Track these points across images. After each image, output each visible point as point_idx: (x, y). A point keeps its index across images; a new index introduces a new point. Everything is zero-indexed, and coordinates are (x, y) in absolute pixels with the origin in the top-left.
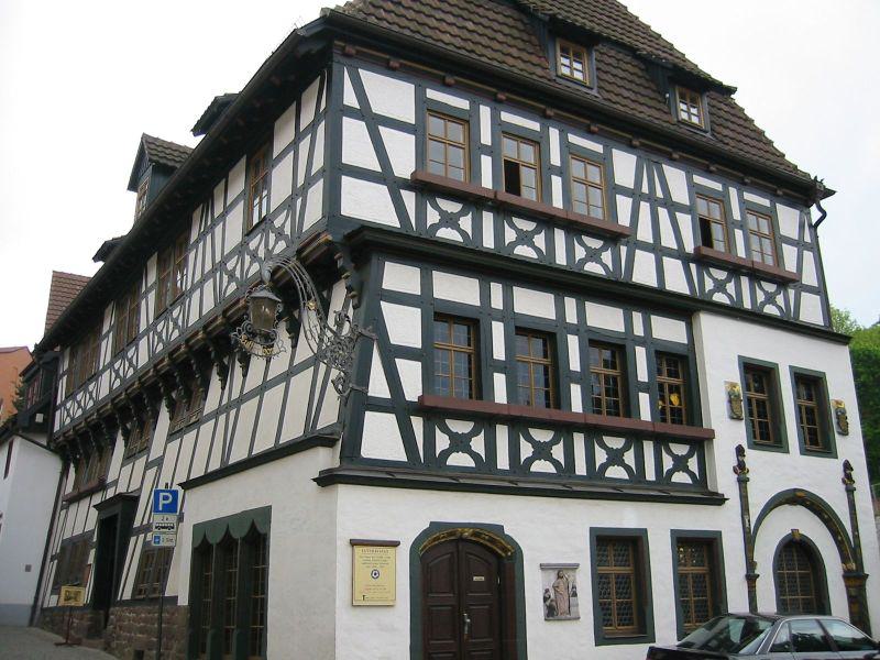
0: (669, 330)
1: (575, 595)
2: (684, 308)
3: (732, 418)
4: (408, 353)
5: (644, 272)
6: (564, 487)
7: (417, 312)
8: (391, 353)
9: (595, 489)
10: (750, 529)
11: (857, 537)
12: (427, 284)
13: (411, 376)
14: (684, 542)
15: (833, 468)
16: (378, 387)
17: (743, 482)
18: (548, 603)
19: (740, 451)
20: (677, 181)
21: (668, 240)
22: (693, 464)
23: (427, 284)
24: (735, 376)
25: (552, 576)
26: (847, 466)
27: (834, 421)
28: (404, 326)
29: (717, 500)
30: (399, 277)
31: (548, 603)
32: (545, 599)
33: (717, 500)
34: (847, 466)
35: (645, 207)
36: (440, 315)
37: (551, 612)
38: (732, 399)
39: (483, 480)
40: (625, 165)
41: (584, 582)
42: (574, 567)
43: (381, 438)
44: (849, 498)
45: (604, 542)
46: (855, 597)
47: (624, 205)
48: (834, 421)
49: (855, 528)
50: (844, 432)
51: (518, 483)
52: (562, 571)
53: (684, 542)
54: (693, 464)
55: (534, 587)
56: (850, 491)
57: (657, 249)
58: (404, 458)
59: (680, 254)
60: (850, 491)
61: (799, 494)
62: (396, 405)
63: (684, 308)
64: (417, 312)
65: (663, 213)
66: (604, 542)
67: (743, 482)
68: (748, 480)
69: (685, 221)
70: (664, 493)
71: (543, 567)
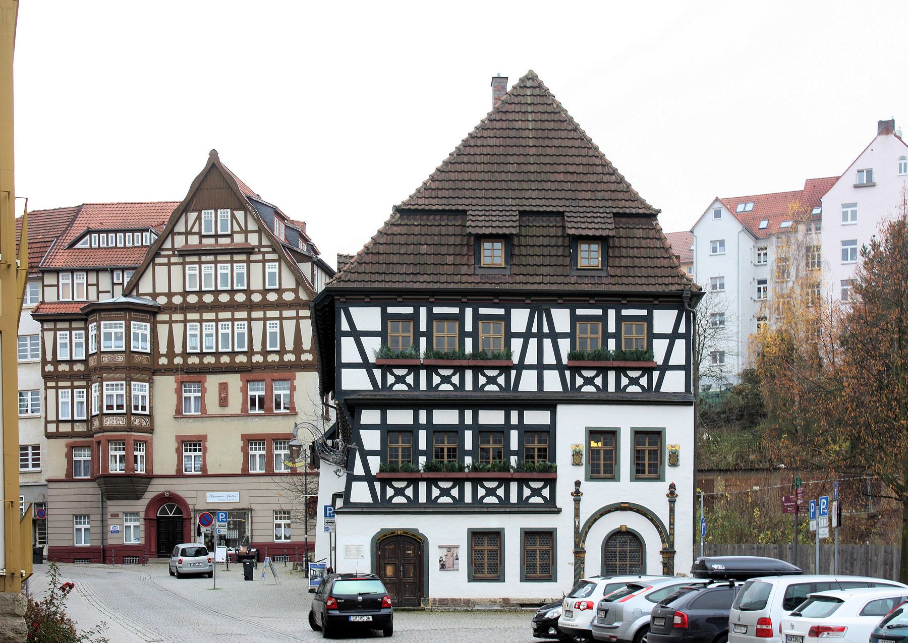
0: (536, 418)
1: (457, 559)
2: (548, 403)
3: (573, 465)
4: (373, 453)
5: (528, 382)
6: (458, 508)
7: (377, 433)
8: (365, 454)
9: (477, 507)
10: (579, 526)
11: (672, 528)
12: (384, 417)
13: (375, 463)
14: (528, 535)
15: (661, 488)
16: (359, 470)
17: (577, 501)
18: (441, 563)
19: (578, 484)
20: (561, 318)
21: (549, 358)
22: (546, 492)
23: (384, 417)
24: (581, 440)
25: (445, 551)
26: (672, 486)
27: (667, 457)
28: (371, 440)
29: (559, 511)
30: (370, 416)
31: (441, 563)
32: (440, 561)
33: (559, 511)
34: (672, 486)
35: (533, 342)
36: (388, 431)
37: (443, 567)
38: (577, 454)
39: (413, 508)
40: (520, 318)
41: (463, 554)
42: (457, 547)
43: (361, 493)
44: (670, 507)
45: (476, 535)
46: (666, 564)
47: (516, 345)
48: (667, 457)
49: (672, 524)
50: (674, 463)
51: (432, 508)
52: (449, 548)
53: (528, 535)
54: (546, 492)
55: (434, 557)
56: (672, 502)
57: (540, 367)
58: (371, 501)
59: (559, 367)
60: (672, 502)
61: (622, 505)
62: (368, 478)
63: (548, 403)
64: (377, 433)
65: (547, 343)
66: (476, 535)
67: (577, 501)
68: (580, 500)
69: (565, 345)
70: (523, 507)
71: (440, 547)
